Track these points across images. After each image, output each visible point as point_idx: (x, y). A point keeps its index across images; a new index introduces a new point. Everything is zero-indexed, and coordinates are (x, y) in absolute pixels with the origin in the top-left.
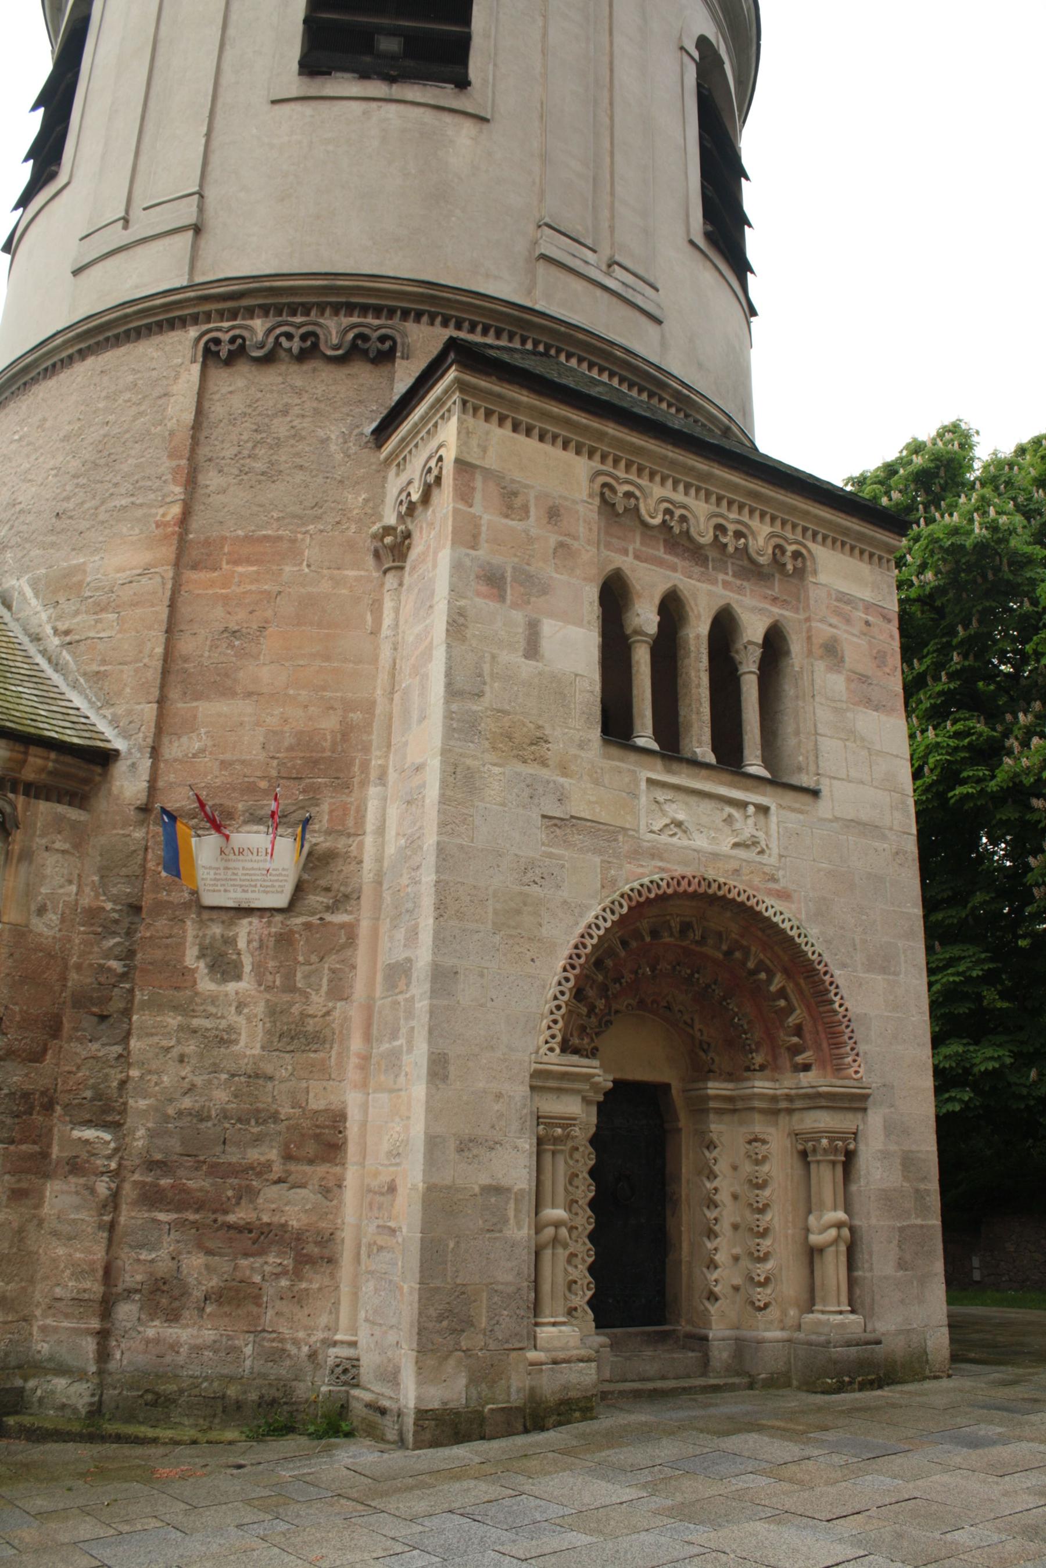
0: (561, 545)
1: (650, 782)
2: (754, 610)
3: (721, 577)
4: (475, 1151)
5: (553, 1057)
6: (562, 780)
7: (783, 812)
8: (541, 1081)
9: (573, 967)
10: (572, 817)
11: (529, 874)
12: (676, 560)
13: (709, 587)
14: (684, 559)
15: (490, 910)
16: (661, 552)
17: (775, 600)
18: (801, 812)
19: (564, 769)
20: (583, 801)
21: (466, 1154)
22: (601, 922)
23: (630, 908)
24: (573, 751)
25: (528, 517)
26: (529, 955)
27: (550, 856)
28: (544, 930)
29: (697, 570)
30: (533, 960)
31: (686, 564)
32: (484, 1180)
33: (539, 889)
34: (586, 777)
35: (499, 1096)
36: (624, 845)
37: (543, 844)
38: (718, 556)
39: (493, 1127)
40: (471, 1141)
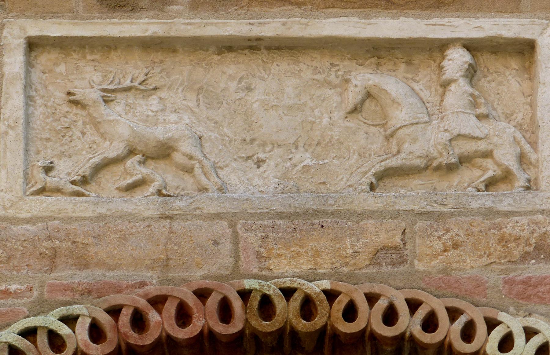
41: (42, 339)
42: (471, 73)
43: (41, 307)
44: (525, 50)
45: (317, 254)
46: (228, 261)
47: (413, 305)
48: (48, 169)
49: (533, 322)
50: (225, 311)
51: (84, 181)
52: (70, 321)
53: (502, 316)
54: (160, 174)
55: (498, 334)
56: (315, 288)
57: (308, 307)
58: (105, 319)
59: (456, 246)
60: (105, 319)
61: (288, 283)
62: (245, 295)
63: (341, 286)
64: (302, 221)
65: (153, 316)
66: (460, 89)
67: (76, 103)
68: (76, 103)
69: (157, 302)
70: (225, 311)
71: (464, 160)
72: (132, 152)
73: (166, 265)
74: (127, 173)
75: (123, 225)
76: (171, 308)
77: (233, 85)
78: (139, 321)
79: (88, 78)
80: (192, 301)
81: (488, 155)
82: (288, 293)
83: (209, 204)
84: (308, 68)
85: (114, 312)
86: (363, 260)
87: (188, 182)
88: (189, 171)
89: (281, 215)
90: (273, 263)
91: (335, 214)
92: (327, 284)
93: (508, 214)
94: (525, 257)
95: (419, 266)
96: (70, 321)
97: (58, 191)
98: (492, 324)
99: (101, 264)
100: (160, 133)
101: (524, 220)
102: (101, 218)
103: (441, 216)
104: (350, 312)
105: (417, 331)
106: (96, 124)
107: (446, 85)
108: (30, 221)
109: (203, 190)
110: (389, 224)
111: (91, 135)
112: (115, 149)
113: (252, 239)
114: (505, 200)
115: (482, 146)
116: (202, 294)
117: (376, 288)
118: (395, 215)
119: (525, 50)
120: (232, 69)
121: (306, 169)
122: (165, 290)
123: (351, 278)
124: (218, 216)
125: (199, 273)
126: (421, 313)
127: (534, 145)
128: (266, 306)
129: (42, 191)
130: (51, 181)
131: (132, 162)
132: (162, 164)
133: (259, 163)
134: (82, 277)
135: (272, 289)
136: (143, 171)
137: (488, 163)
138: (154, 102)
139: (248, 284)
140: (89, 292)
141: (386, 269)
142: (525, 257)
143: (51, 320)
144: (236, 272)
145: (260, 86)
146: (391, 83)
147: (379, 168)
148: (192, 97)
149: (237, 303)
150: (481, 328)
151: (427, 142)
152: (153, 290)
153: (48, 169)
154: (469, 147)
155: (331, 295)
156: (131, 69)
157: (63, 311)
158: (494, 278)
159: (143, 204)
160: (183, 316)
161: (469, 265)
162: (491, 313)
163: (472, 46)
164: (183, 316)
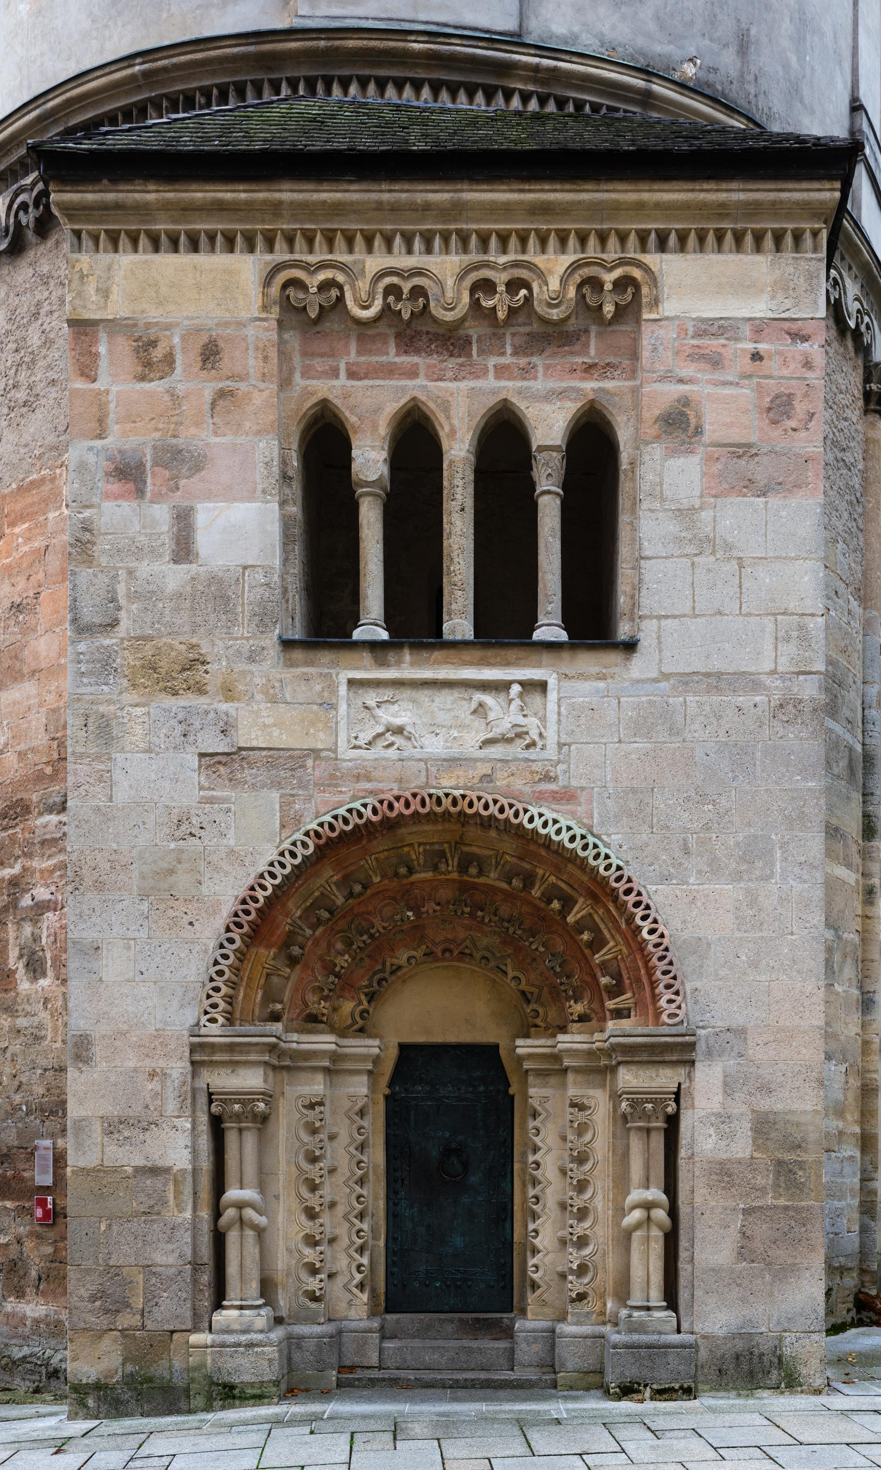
0: (222, 394)
1: (351, 682)
2: (549, 396)
3: (492, 361)
4: (126, 1134)
5: (214, 1029)
6: (224, 707)
7: (566, 684)
8: (201, 1055)
9: (239, 925)
10: (241, 749)
11: (183, 828)
12: (416, 359)
13: (472, 384)
14: (430, 354)
15: (135, 874)
16: (392, 355)
17: (589, 368)
18: (602, 677)
19: (228, 692)
20: (260, 725)
21: (116, 1136)
22: (277, 870)
23: (317, 846)
24: (241, 666)
25: (173, 370)
26: (187, 919)
27: (211, 801)
28: (204, 889)
29: (452, 363)
30: (191, 924)
31: (434, 360)
32: (140, 1162)
33: (195, 841)
34: (259, 697)
35: (152, 1075)
36: (314, 770)
37: (201, 788)
38: (489, 331)
39: (147, 1107)
40: (121, 1123)
41: (355, 813)
42: (521, 695)
43: (354, 799)
44: (542, 686)
45: (458, 777)
46: (424, 780)
47: (495, 802)
48: (356, 738)
49: (543, 810)
50: (423, 803)
51: (370, 743)
52: (365, 806)
53: (530, 808)
54: (399, 741)
55: (528, 815)
56: (457, 793)
57: (455, 802)
58: (378, 805)
59: (513, 775)
60: (378, 805)
61: (447, 791)
62: (430, 796)
63: (468, 793)
64: (453, 762)
65: (396, 805)
66: (517, 702)
67: (366, 708)
68: (366, 708)
69: (398, 798)
70: (423, 803)
71: (519, 735)
72: (388, 730)
73: (400, 781)
74: (386, 740)
75: (384, 763)
76: (402, 801)
77: (427, 699)
78: (391, 807)
79: (371, 698)
80: (410, 798)
81: (527, 733)
82: (447, 795)
83: (417, 753)
84: (456, 693)
85: (381, 802)
86: (476, 781)
87: (409, 744)
88: (409, 739)
89: (445, 760)
90: (441, 781)
91: (465, 759)
92: (462, 792)
93: (534, 761)
94: (540, 780)
95: (498, 783)
96: (365, 806)
97: (360, 747)
98: (526, 811)
99: (376, 780)
100: (398, 721)
101: (540, 764)
102: (376, 759)
103: (507, 761)
104: (471, 805)
105: (496, 813)
106: (374, 717)
107: (511, 701)
108: (349, 761)
109: (415, 747)
110: (487, 765)
111: (372, 722)
112: (380, 729)
113: (433, 770)
114: (532, 754)
115: (524, 729)
116: (414, 795)
117: (481, 794)
118: (490, 760)
119: (542, 686)
120: (426, 692)
121: (455, 738)
122: (401, 793)
123: (471, 788)
124: (420, 760)
125: (413, 785)
126: (498, 805)
127: (545, 727)
128: (439, 801)
129: (355, 747)
130: (357, 743)
131: (388, 735)
132: (399, 736)
133: (437, 734)
134: (369, 786)
135: (440, 793)
136: (393, 739)
137: (527, 737)
138: (396, 707)
139: (432, 791)
140: (371, 792)
141: (485, 785)
142: (540, 780)
143: (357, 805)
144: (427, 785)
145: (437, 700)
146: (488, 699)
147: (483, 738)
148: (411, 704)
149: (427, 799)
150: (521, 812)
151: (503, 727)
152: (396, 792)
153: (356, 738)
154: (520, 730)
155: (464, 797)
156: (387, 694)
157: (362, 801)
158: (527, 789)
159: (392, 753)
160: (407, 805)
161: (519, 784)
162: (526, 806)
163: (521, 683)
164: (407, 805)
